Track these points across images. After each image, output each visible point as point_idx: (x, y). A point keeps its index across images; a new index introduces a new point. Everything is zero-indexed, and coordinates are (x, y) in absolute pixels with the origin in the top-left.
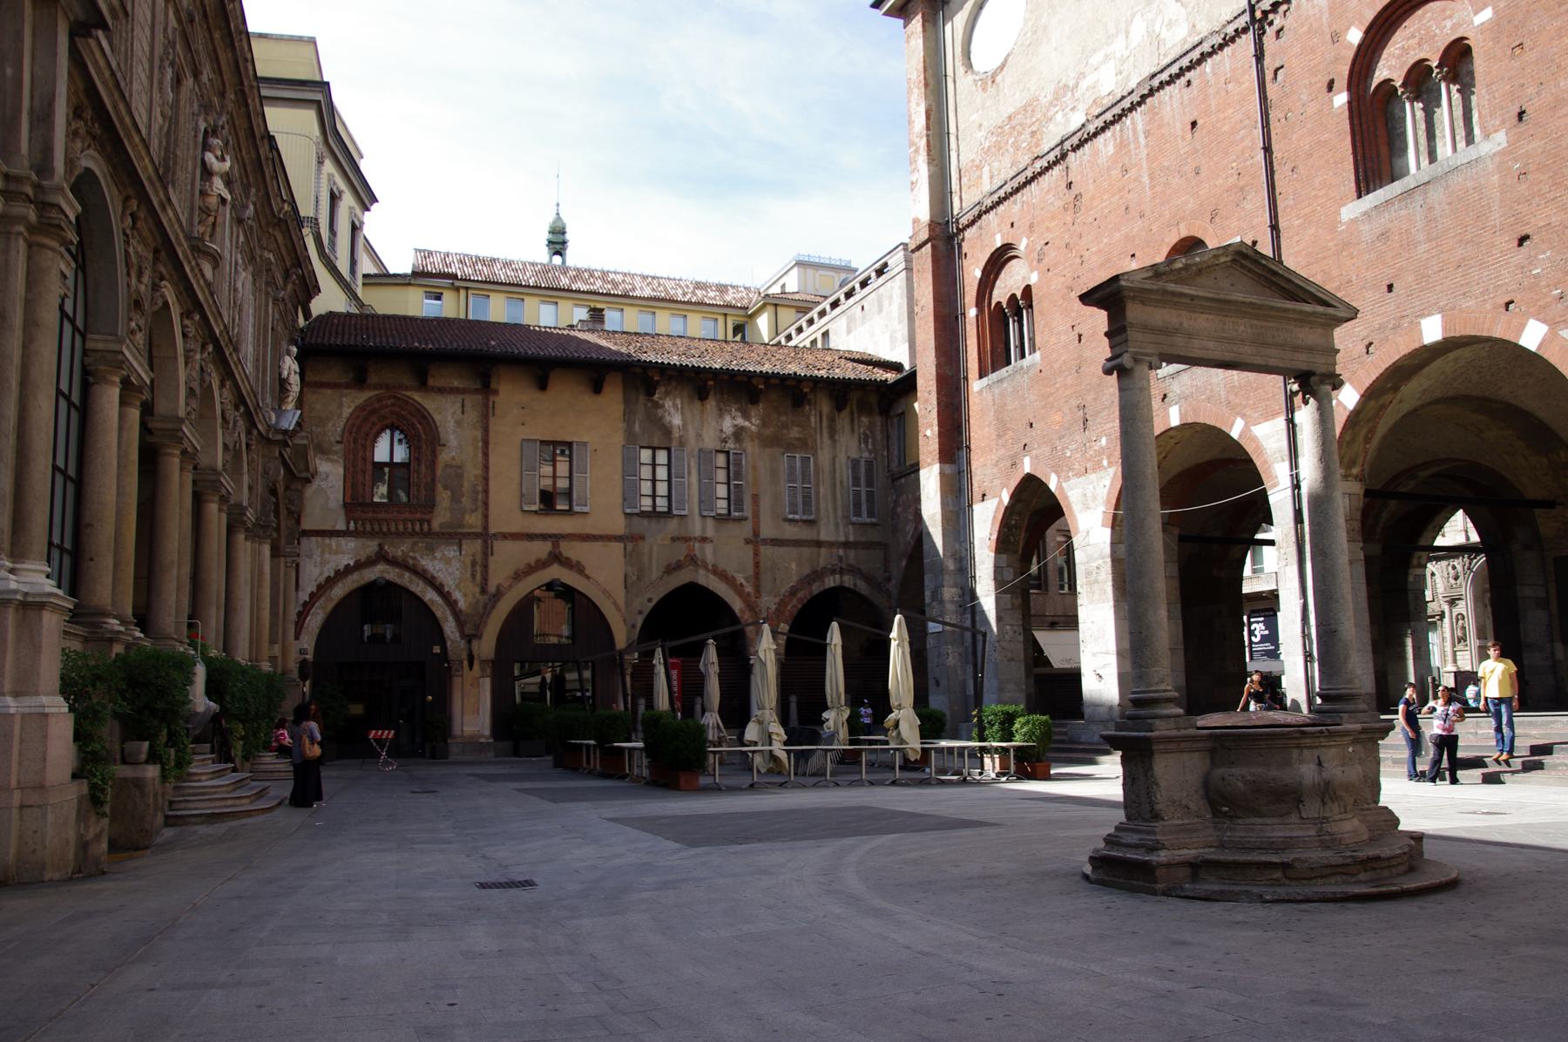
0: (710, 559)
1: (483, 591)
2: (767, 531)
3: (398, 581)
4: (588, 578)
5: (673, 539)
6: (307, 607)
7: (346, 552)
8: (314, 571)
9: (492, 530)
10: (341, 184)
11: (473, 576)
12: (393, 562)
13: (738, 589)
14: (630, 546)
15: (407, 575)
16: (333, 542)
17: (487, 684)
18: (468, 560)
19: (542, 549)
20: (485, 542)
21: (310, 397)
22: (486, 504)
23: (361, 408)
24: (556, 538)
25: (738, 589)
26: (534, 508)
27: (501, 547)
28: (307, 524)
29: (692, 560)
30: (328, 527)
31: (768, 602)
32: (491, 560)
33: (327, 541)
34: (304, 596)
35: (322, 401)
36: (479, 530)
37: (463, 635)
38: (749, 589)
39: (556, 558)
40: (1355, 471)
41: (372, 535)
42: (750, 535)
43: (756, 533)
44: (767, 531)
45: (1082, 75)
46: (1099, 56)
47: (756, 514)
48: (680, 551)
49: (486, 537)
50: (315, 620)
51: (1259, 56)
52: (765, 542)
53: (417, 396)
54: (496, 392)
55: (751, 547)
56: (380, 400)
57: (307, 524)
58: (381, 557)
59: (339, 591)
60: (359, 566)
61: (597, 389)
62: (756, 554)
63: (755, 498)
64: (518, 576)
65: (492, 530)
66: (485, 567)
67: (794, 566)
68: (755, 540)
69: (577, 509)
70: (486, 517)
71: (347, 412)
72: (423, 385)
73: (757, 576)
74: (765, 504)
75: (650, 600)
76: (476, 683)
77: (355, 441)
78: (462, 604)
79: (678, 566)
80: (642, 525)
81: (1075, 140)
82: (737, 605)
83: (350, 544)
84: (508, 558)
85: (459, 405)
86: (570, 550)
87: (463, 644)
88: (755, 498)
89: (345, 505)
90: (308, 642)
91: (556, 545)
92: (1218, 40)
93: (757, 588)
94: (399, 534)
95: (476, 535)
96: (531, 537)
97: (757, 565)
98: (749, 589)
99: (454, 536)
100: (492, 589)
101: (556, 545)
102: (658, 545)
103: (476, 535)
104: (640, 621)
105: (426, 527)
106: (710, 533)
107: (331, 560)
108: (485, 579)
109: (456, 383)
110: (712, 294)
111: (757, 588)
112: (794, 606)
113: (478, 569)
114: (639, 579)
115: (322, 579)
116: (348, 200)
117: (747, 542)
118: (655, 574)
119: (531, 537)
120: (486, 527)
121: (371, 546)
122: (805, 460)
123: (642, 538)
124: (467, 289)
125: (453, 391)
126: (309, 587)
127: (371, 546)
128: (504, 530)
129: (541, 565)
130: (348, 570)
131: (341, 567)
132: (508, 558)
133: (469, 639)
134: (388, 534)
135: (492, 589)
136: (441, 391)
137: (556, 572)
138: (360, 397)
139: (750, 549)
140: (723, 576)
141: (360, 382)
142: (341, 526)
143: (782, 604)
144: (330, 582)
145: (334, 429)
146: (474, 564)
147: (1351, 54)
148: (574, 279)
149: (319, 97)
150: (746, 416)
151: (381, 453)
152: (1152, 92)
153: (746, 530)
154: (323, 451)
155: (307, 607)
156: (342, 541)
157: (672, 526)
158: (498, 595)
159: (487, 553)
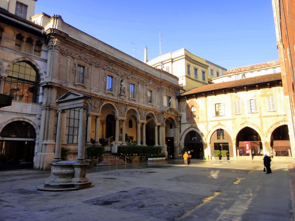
1: (208, 131)
3: (194, 130)
4: (225, 127)
6: (182, 135)
7: (187, 126)
8: (183, 130)
10: (197, 66)
11: (206, 128)
12: (194, 127)
13: (257, 127)
14: (233, 121)
15: (196, 129)
16: (185, 125)
19: (217, 123)
20: (207, 123)
22: (207, 116)
27: (210, 123)
28: (182, 122)
30: (184, 123)
32: (208, 126)
33: (184, 125)
34: (182, 133)
36: (206, 120)
41: (190, 123)
42: (259, 116)
43: (261, 115)
47: (260, 111)
48: (244, 121)
52: (263, 117)
55: (260, 118)
56: (190, 102)
58: (192, 127)
59: (186, 132)
60: (189, 128)
62: (261, 119)
63: (260, 108)
65: (208, 120)
66: (207, 127)
68: (261, 117)
73: (262, 124)
75: (238, 131)
77: (188, 109)
80: (235, 117)
83: (187, 125)
86: (221, 122)
88: (260, 108)
91: (219, 122)
93: (262, 126)
97: (262, 122)
99: (203, 122)
105: (198, 121)
108: (207, 129)
114: (235, 126)
115: (184, 131)
120: (207, 120)
121: (190, 125)
122: (272, 98)
127: (190, 125)
130: (187, 129)
131: (187, 129)
135: (209, 131)
142: (186, 122)
144: (185, 131)
153: (258, 115)
154: (183, 111)
155: (182, 135)
157: (241, 116)
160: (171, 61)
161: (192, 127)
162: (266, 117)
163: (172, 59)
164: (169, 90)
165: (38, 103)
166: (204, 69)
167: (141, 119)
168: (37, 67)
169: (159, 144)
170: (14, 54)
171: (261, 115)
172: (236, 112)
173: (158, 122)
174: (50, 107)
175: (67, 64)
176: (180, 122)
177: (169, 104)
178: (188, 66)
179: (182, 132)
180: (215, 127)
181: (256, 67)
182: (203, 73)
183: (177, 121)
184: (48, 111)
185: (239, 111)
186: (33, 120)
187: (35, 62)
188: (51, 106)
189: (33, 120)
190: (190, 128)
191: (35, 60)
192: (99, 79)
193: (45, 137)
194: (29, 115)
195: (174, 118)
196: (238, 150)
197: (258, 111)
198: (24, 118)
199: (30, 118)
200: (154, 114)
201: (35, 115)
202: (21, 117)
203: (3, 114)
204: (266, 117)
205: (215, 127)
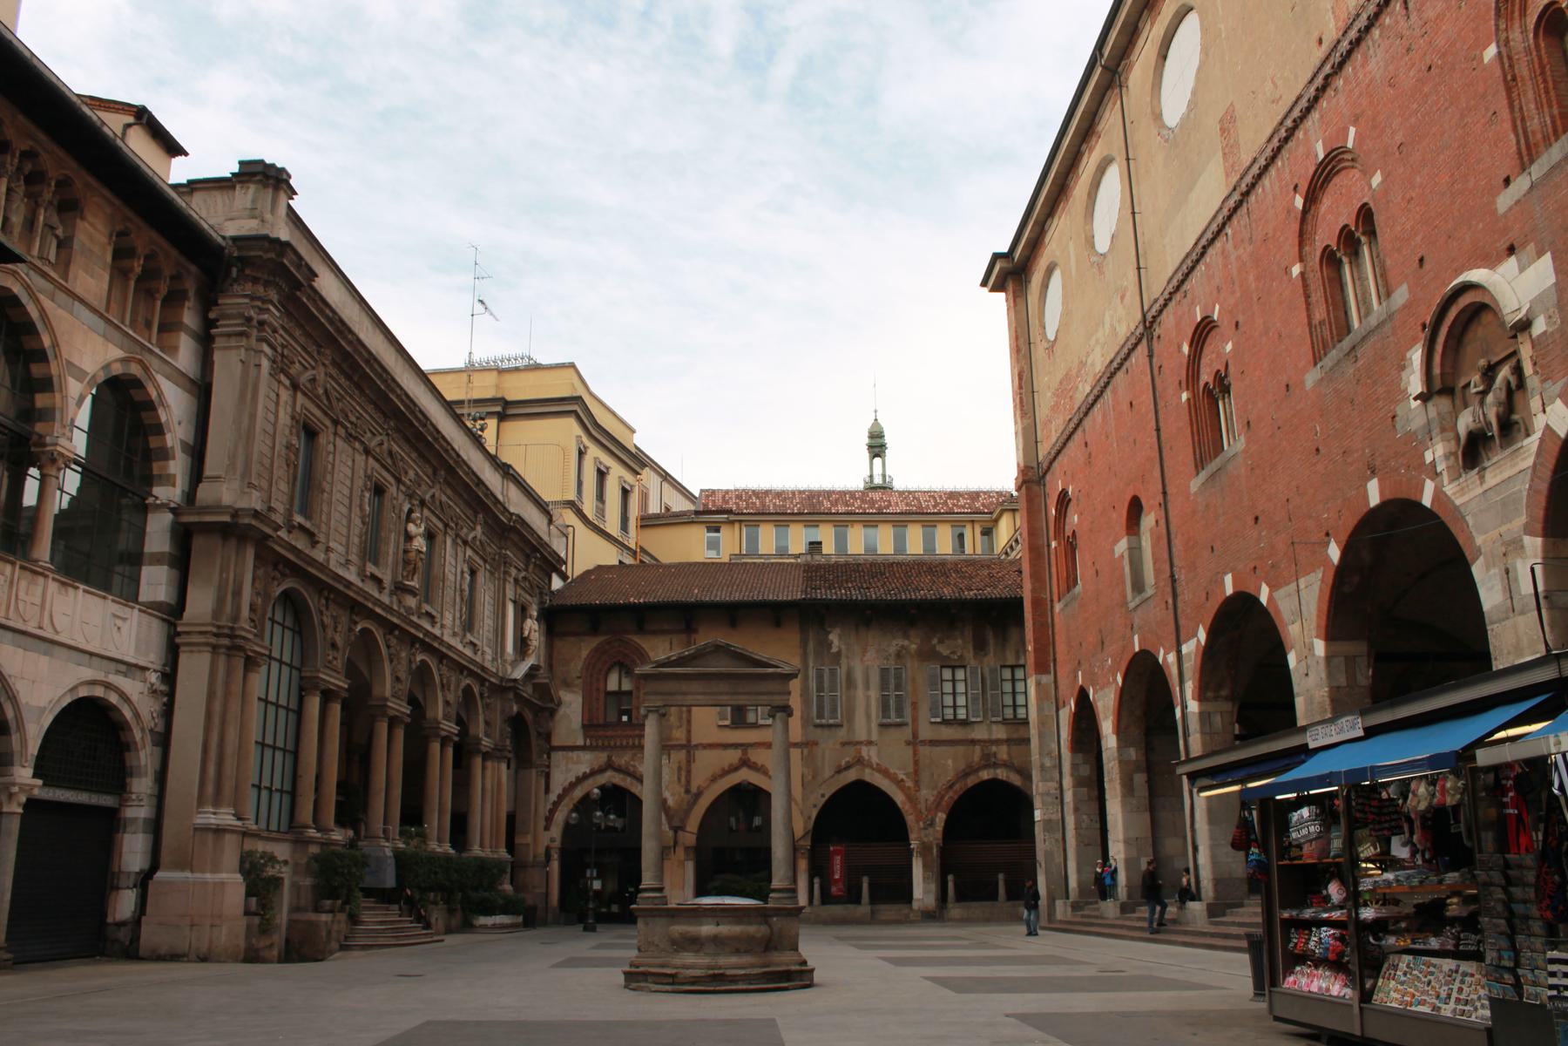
0: (875, 760)
1: (687, 791)
2: (926, 732)
3: (622, 784)
5: (844, 744)
6: (556, 804)
7: (584, 762)
8: (560, 780)
9: (694, 742)
10: (607, 460)
12: (619, 770)
13: (899, 783)
16: (574, 755)
17: (690, 867)
18: (675, 767)
19: (733, 756)
21: (558, 644)
22: (689, 722)
23: (596, 650)
24: (744, 747)
25: (899, 783)
26: (727, 722)
28: (556, 742)
29: (859, 761)
31: (927, 795)
32: (694, 766)
34: (553, 797)
35: (565, 646)
37: (671, 827)
38: (909, 784)
39: (745, 763)
40: (1224, 693)
41: (603, 748)
43: (915, 735)
44: (926, 732)
45: (1088, 354)
46: (1092, 342)
47: (915, 720)
49: (689, 747)
50: (560, 817)
51: (1151, 356)
52: (923, 742)
53: (637, 639)
54: (696, 631)
57: (556, 742)
58: (609, 766)
60: (593, 773)
61: (778, 623)
62: (915, 754)
63: (914, 704)
64: (714, 779)
65: (694, 742)
66: (689, 772)
67: (950, 762)
68: (914, 742)
69: (761, 722)
70: (689, 732)
71: (585, 653)
72: (641, 629)
73: (916, 772)
74: (924, 710)
76: (682, 864)
78: (670, 802)
79: (848, 767)
81: (1084, 409)
82: (899, 798)
84: (706, 763)
85: (667, 645)
86: (757, 756)
87: (671, 833)
88: (914, 704)
89: (584, 726)
90: (556, 832)
91: (745, 752)
92: (1133, 340)
93: (917, 783)
94: (623, 748)
95: (682, 747)
96: (726, 746)
97: (916, 763)
98: (909, 784)
100: (694, 789)
101: (745, 752)
102: (830, 750)
103: (682, 747)
104: (814, 814)
106: (874, 737)
107: (573, 768)
108: (688, 782)
109: (666, 627)
110: (962, 502)
111: (917, 783)
112: (951, 797)
113: (684, 773)
116: (617, 472)
117: (908, 743)
118: (828, 772)
119: (726, 746)
120: (689, 740)
121: (602, 757)
123: (816, 744)
124: (740, 521)
125: (663, 632)
126: (557, 789)
127: (602, 757)
128: (705, 741)
129: (734, 769)
130: (585, 777)
132: (706, 763)
133: (676, 830)
134: (615, 747)
135: (694, 789)
136: (654, 633)
137: (745, 775)
138: (594, 642)
139: (910, 750)
140: (885, 773)
141: (594, 630)
142: (580, 742)
143: (941, 797)
145: (576, 667)
146: (680, 769)
147: (1185, 361)
148: (835, 503)
149: (575, 407)
150: (906, 636)
151: (612, 685)
152: (1113, 375)
153: (908, 731)
154: (567, 685)
155: (556, 804)
156: (581, 753)
157: (842, 734)
158: (698, 795)
159: (690, 760)
160: (498, 409)
161: (609, 766)
162: (934, 743)
163: (507, 404)
164: (523, 574)
165: (136, 601)
166: (629, 477)
167: (446, 717)
168: (161, 411)
169: (482, 845)
170: (100, 340)
171: (915, 735)
172: (820, 716)
173: (487, 735)
174: (232, 636)
175: (277, 417)
176: (548, 737)
177: (522, 644)
178: (581, 454)
179: (557, 789)
180: (725, 773)
181: (827, 504)
182: (625, 493)
183: (539, 734)
184: (222, 660)
185: (834, 711)
186: (135, 698)
187: (158, 388)
188: (238, 633)
189: (136, 698)
190: (601, 770)
191: (160, 379)
192: (350, 498)
193: (210, 789)
194: (123, 668)
195: (529, 716)
196: (817, 881)
197: (908, 718)
198: (108, 686)
199: (133, 687)
200: (476, 690)
201: (144, 669)
202: (100, 676)
203: (51, 656)
204: (934, 743)
205: (725, 773)
